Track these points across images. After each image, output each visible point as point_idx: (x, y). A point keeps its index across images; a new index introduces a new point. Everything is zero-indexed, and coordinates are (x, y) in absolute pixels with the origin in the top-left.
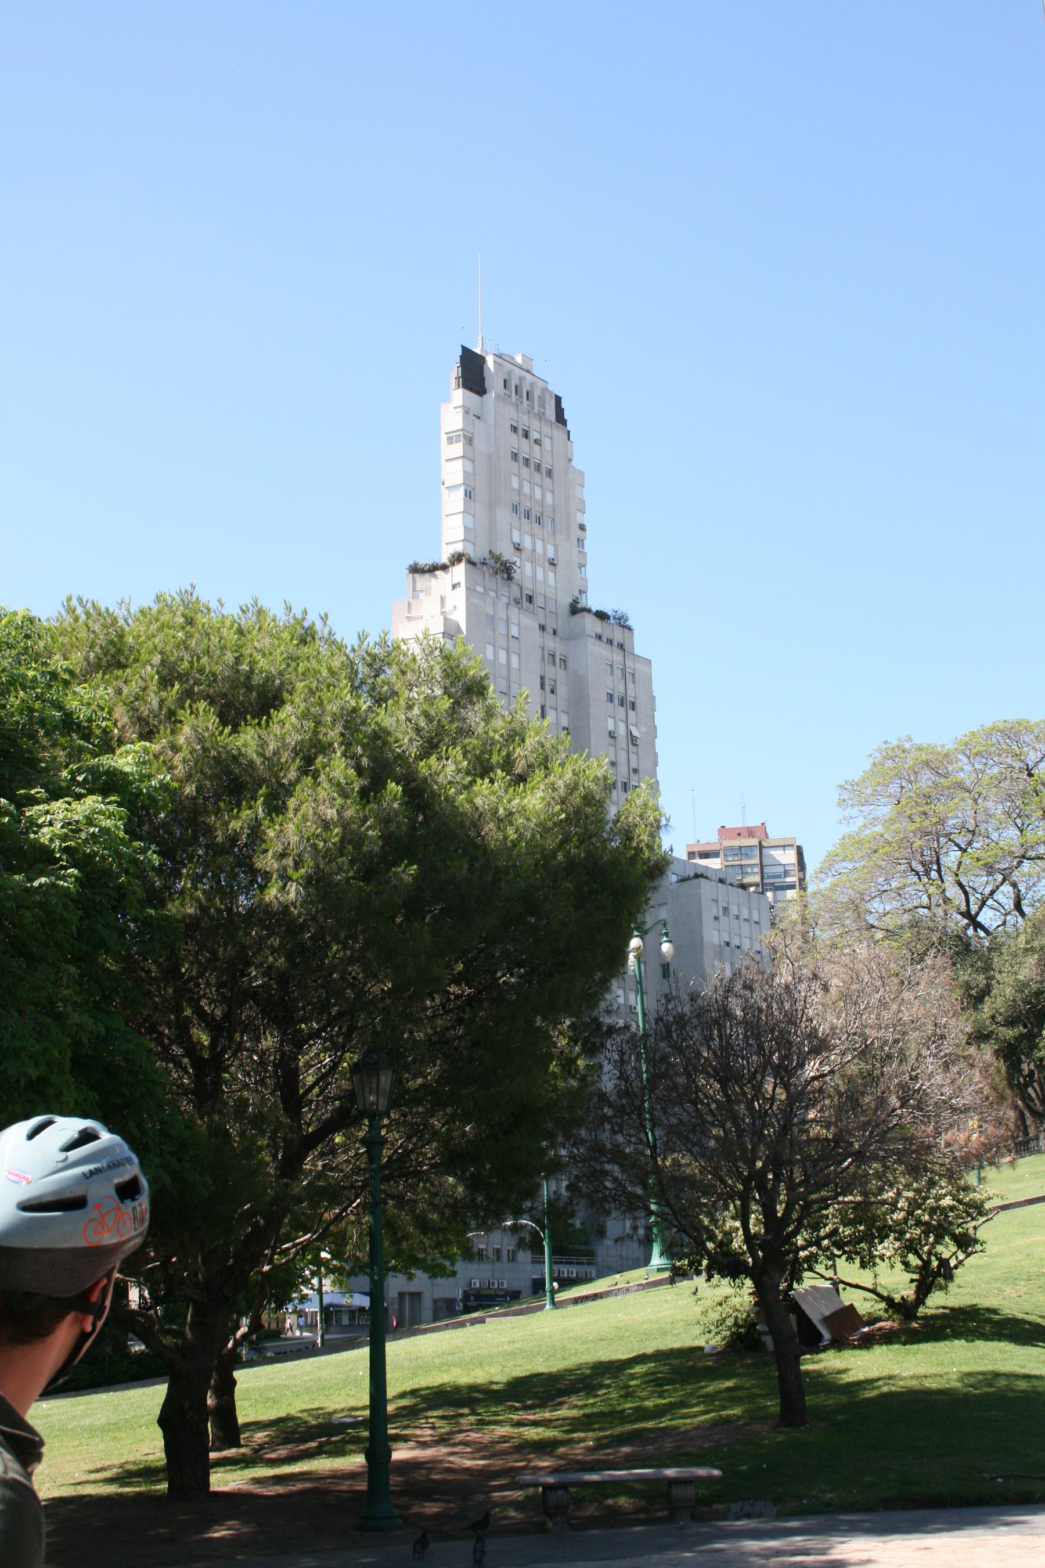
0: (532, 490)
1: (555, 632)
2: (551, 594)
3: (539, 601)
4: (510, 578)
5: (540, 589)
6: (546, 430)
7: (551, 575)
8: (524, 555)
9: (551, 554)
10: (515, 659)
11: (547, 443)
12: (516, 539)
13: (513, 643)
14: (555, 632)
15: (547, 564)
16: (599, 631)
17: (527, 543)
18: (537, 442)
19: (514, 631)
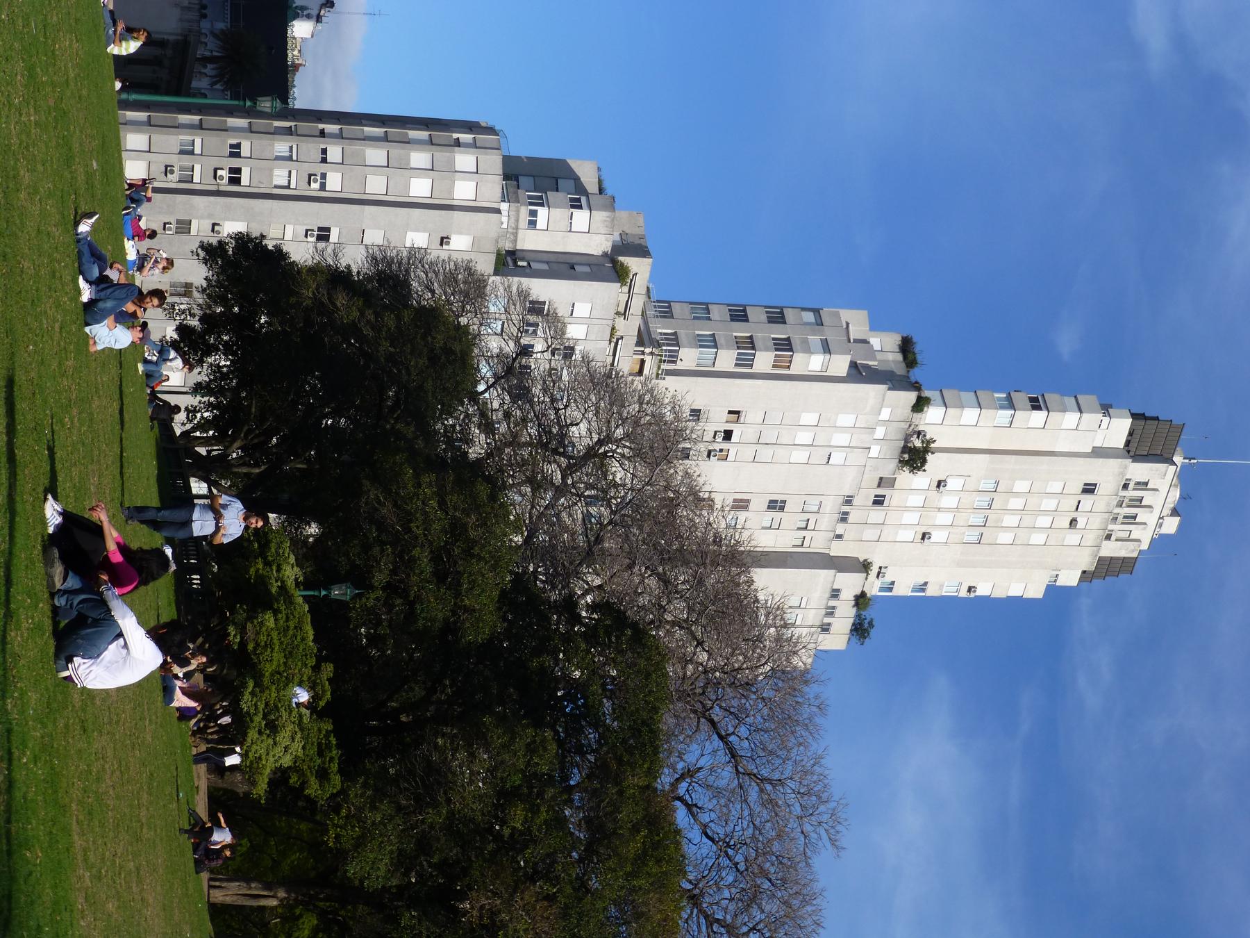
0: (1013, 511)
1: (839, 537)
2: (887, 534)
3: (877, 514)
4: (903, 463)
5: (893, 517)
6: (1091, 538)
7: (908, 535)
8: (933, 493)
9: (937, 536)
10: (799, 456)
11: (1073, 538)
12: (953, 484)
13: (821, 454)
14: (839, 537)
15: (924, 530)
16: (843, 596)
17: (948, 500)
18: (1073, 522)
19: (837, 458)
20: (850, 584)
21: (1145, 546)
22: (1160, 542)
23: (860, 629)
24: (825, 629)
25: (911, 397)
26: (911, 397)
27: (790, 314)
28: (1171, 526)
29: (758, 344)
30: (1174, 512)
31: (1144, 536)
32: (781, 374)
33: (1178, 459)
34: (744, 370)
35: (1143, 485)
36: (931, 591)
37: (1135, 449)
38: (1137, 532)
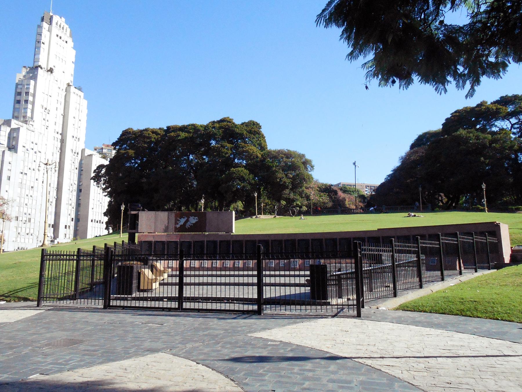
20: (72, 89)
21: (68, 27)
22: (66, 22)
23: (80, 89)
24: (80, 96)
25: (39, 68)
26: (39, 68)
27: (19, 91)
28: (63, 19)
29: (26, 99)
30: (61, 18)
31: (66, 26)
32: (34, 96)
33: (51, 14)
34: (33, 103)
35: (57, 24)
36: (73, 74)
37: (50, 23)
38: (65, 28)
